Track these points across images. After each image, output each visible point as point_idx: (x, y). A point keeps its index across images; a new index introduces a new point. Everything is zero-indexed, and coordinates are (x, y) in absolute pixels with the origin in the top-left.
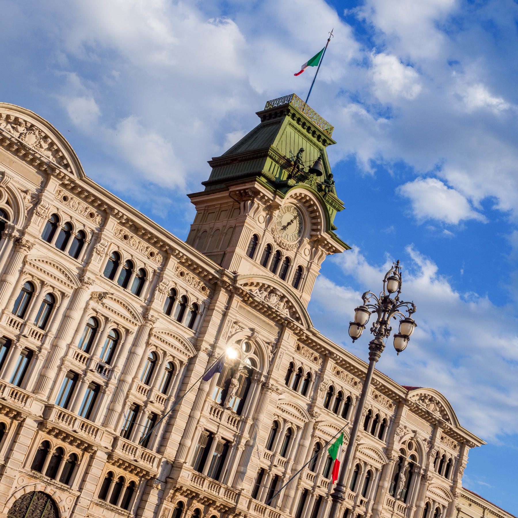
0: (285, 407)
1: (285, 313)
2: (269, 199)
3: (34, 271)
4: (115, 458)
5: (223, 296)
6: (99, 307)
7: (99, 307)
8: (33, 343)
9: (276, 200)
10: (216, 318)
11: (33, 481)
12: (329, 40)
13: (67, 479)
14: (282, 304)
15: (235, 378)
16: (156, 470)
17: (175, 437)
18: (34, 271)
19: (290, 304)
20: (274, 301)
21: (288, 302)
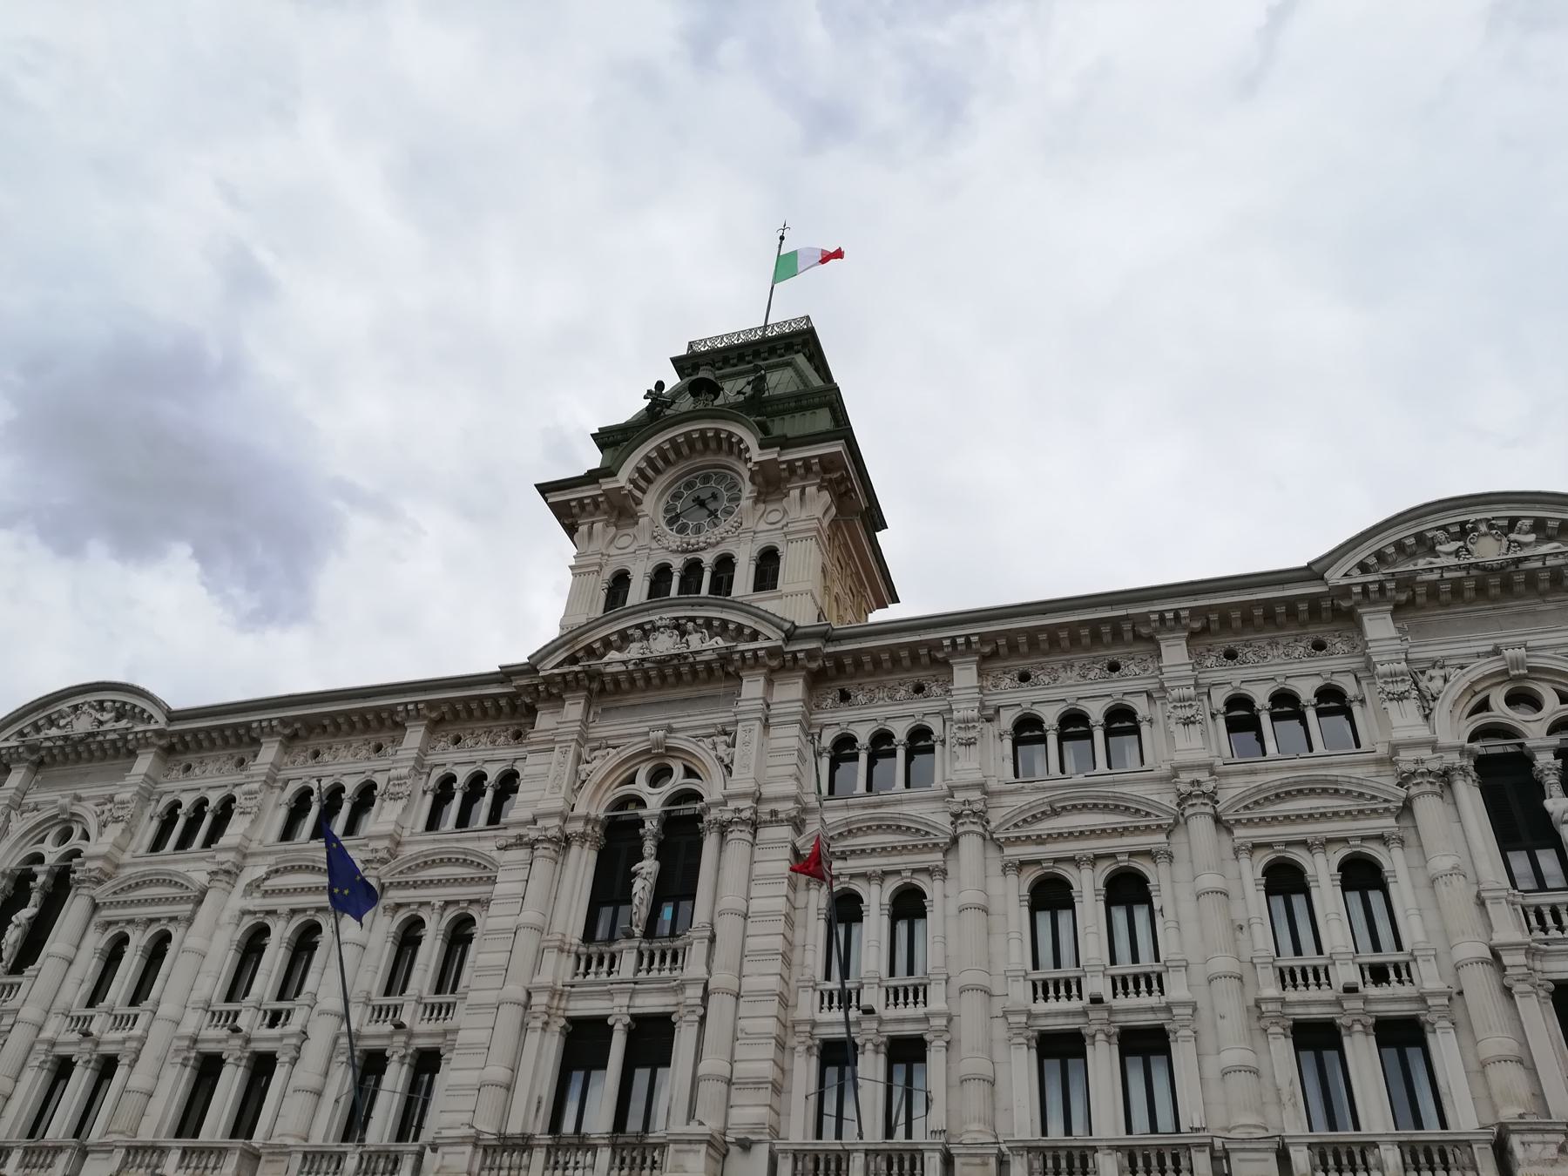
2: (594, 498)
5: (544, 720)
6: (256, 902)
12: (782, 238)
15: (641, 858)
20: (664, 644)
21: (708, 622)
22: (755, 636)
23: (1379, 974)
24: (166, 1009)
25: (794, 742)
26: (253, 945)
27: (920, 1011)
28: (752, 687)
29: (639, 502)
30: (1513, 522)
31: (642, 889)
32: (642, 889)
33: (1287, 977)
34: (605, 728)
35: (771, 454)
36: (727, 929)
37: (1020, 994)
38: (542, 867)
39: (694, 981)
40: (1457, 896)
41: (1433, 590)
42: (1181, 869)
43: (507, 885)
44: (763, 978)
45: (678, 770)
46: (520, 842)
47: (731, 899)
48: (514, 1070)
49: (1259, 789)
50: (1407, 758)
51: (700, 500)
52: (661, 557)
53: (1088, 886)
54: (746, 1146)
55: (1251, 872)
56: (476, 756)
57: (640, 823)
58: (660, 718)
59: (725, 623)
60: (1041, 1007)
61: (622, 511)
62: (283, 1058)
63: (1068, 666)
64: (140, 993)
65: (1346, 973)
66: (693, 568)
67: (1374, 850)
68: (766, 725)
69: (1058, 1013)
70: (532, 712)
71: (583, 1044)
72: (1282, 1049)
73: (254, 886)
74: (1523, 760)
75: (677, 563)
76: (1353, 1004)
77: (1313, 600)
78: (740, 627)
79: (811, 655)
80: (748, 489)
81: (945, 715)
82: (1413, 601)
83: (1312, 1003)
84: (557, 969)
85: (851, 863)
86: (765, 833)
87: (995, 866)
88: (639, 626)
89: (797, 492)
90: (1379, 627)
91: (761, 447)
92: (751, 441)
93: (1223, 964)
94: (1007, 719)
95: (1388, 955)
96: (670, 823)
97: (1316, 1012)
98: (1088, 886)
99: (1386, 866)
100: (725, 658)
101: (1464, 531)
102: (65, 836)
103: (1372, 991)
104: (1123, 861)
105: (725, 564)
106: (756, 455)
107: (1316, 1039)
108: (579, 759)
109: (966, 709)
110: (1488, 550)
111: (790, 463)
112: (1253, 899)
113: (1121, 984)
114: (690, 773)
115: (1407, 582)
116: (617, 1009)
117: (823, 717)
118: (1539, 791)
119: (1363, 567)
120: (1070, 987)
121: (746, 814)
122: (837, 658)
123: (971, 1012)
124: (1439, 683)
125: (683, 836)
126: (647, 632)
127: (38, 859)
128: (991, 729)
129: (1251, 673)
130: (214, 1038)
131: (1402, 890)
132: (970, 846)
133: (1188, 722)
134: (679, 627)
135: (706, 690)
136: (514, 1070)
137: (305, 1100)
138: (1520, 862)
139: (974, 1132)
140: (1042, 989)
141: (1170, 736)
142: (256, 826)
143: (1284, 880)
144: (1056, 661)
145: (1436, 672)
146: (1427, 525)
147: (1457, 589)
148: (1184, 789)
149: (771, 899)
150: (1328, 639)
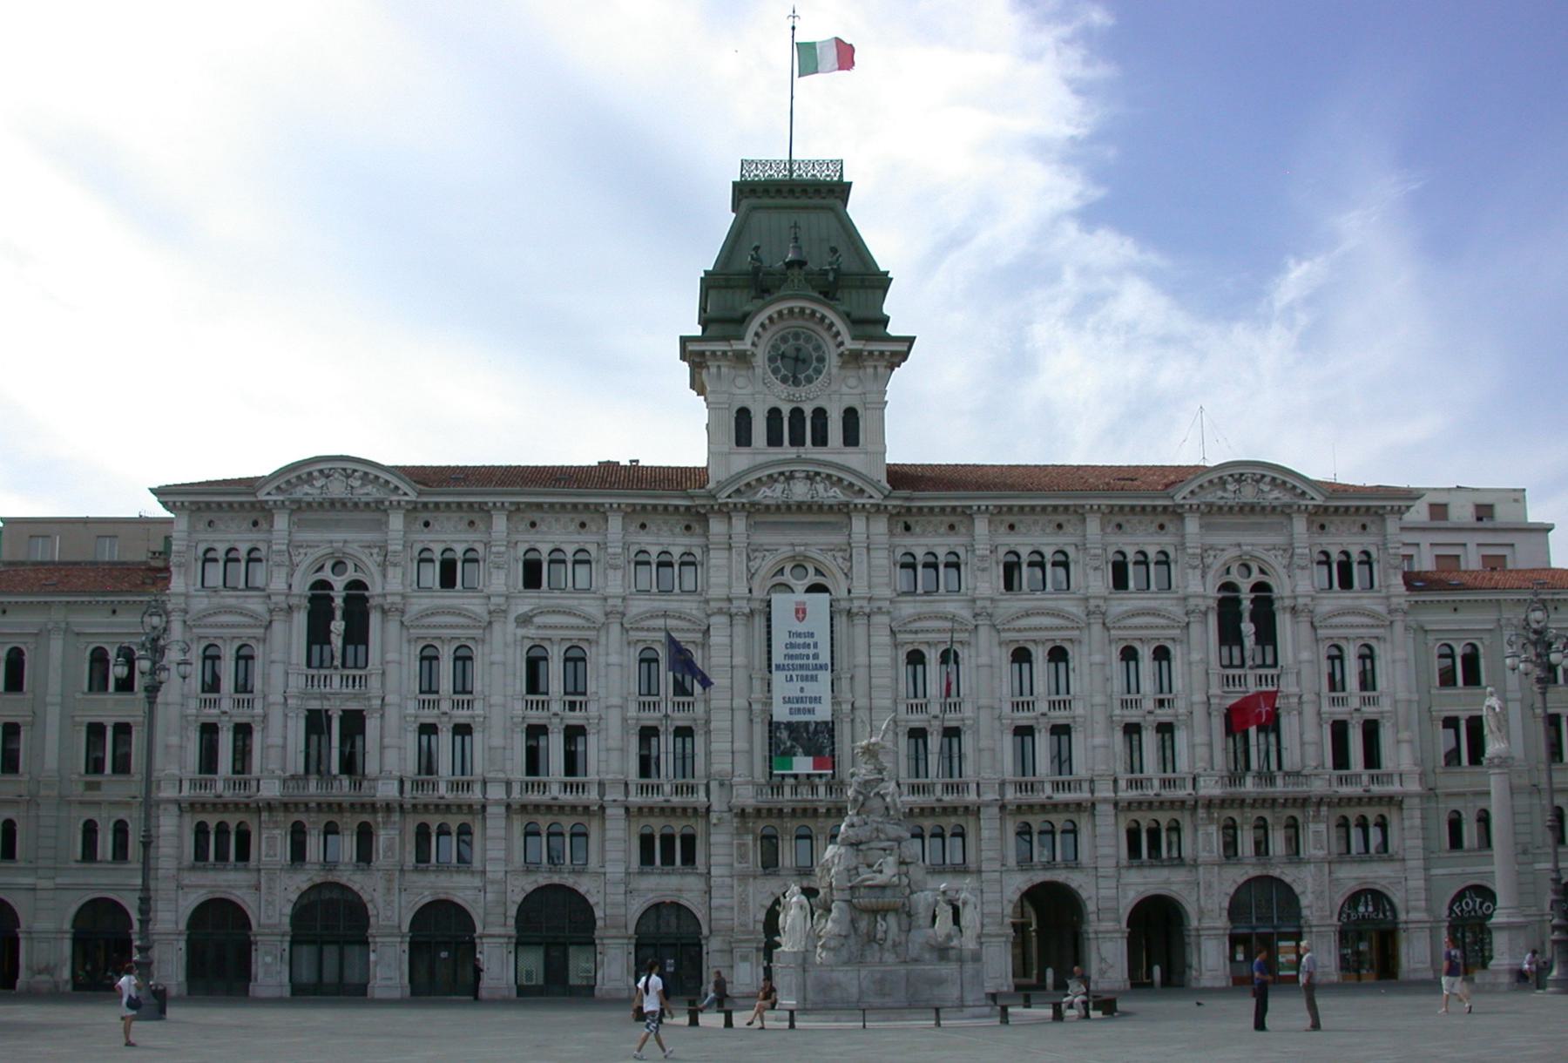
2: (725, 353)
4: (634, 810)
5: (717, 526)
6: (531, 632)
7: (531, 632)
10: (717, 558)
11: (532, 878)
14: (820, 487)
17: (720, 745)
20: (800, 491)
21: (829, 476)
22: (862, 491)
23: (1161, 703)
24: (496, 699)
25: (885, 562)
27: (959, 715)
28: (858, 524)
29: (753, 355)
30: (1263, 476)
33: (1125, 704)
34: (764, 538)
35: (858, 345)
36: (861, 674)
37: (1007, 708)
38: (739, 629)
40: (1198, 671)
41: (1220, 508)
42: (1085, 649)
43: (718, 638)
44: (883, 700)
45: (811, 571)
46: (720, 612)
47: (861, 659)
48: (751, 742)
50: (1192, 602)
51: (795, 363)
53: (1040, 654)
55: (1115, 653)
56: (662, 540)
58: (797, 537)
59: (840, 480)
60: (1016, 715)
61: (743, 358)
62: (591, 730)
63: (1036, 522)
65: (1149, 704)
66: (797, 413)
67: (1169, 645)
68: (868, 549)
69: (1023, 718)
70: (704, 519)
72: (1119, 735)
73: (524, 620)
74: (1237, 602)
75: (786, 410)
76: (1150, 718)
77: (1165, 508)
78: (851, 485)
80: (833, 360)
81: (970, 548)
82: (1211, 513)
83: (1133, 716)
86: (876, 619)
87: (995, 641)
88: (782, 474)
90: (1192, 525)
91: (854, 338)
92: (840, 326)
93: (1098, 699)
95: (1164, 696)
97: (1134, 720)
98: (1040, 654)
99: (1173, 652)
101: (1239, 479)
102: (338, 566)
103: (1158, 711)
105: (820, 414)
106: (850, 345)
107: (1132, 730)
109: (982, 548)
110: (1248, 494)
111: (871, 353)
112: (1117, 666)
113: (1053, 705)
114: (818, 572)
115: (1210, 505)
117: (897, 540)
119: (1192, 492)
120: (1028, 705)
121: (867, 610)
122: (909, 509)
123: (984, 716)
126: (791, 477)
127: (324, 585)
128: (994, 557)
130: (536, 717)
131: (1177, 665)
132: (984, 632)
133: (1096, 569)
134: (810, 478)
135: (824, 518)
136: (751, 742)
137: (615, 755)
138: (1225, 650)
139: (986, 774)
140: (1016, 706)
141: (1086, 575)
143: (1129, 654)
144: (1029, 519)
145: (1212, 553)
146: (1225, 473)
147: (1231, 508)
148: (1092, 608)
149: (882, 657)
150: (1167, 524)
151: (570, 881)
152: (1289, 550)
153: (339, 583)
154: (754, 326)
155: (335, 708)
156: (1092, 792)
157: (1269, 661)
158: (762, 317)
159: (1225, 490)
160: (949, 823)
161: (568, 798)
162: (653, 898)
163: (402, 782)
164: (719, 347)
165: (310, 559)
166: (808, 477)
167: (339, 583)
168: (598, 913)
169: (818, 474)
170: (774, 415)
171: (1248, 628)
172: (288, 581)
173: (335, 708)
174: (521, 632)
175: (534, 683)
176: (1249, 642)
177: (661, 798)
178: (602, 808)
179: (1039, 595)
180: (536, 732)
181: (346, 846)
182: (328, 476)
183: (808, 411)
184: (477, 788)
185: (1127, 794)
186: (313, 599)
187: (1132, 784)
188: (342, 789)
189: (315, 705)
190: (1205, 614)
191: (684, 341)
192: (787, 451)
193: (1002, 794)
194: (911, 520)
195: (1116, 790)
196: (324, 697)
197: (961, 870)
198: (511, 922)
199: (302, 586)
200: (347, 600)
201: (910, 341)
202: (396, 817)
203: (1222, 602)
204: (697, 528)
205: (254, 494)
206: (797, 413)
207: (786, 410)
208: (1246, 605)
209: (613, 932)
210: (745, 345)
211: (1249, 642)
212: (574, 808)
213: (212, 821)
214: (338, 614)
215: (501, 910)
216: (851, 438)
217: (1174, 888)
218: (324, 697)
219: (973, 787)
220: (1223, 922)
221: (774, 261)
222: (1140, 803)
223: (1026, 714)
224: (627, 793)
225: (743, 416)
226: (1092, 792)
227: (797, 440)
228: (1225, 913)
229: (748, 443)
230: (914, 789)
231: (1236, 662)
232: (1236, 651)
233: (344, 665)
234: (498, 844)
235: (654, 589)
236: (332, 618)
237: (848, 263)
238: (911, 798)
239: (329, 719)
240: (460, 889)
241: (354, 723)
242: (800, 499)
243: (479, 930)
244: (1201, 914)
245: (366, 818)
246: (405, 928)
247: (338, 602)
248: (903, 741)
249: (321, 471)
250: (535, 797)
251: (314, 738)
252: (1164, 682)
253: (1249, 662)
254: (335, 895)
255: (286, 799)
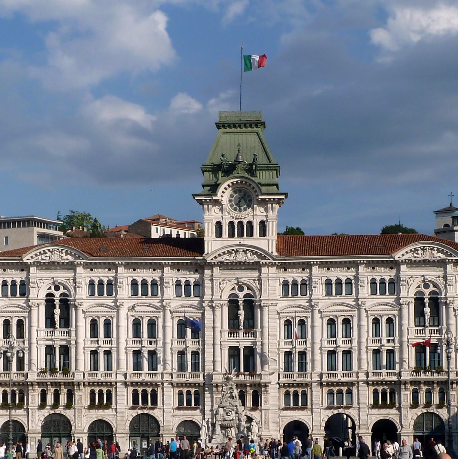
0: (289, 310)
1: (256, 259)
3: (91, 314)
4: (175, 384)
6: (134, 314)
7: (134, 314)
8: (107, 347)
9: (214, 198)
10: (207, 284)
13: (154, 402)
14: (249, 255)
15: (240, 310)
16: (201, 379)
17: (209, 358)
18: (91, 314)
19: (254, 252)
20: (241, 257)
21: (252, 251)
23: (389, 341)
26: (137, 324)
30: (434, 247)
31: (242, 318)
32: (242, 318)
39: (259, 341)
49: (374, 304)
52: (231, 219)
54: (273, 373)
57: (238, 302)
61: (217, 203)
64: (108, 334)
66: (241, 223)
71: (234, 352)
75: (236, 222)
79: (279, 263)
84: (226, 336)
85: (289, 314)
88: (233, 250)
89: (270, 205)
92: (256, 188)
94: (324, 279)
96: (244, 301)
100: (257, 263)
104: (347, 317)
105: (250, 223)
108: (220, 284)
116: (242, 345)
118: (424, 306)
124: (412, 281)
125: (250, 305)
126: (237, 251)
129: (377, 274)
134: (245, 252)
142: (124, 291)
151: (151, 412)
152: (445, 278)
153: (57, 294)
154: (221, 189)
155: (57, 345)
156: (358, 377)
157: (436, 324)
158: (225, 185)
159: (418, 254)
160: (300, 390)
161: (149, 379)
162: (183, 419)
163: (84, 374)
164: (208, 199)
165: (46, 284)
166: (243, 251)
167: (57, 294)
168: (161, 424)
169: (247, 250)
170: (231, 224)
171: (427, 310)
172: (39, 293)
173: (57, 345)
174: (130, 313)
175: (137, 333)
176: (428, 316)
177: (185, 380)
178: (163, 384)
179: (338, 297)
180: (137, 354)
181: (63, 399)
182: (51, 252)
183: (245, 222)
184: (114, 376)
185: (372, 378)
186: (46, 301)
187: (375, 374)
188: (59, 377)
189: (50, 343)
190: (408, 305)
191: (194, 196)
192: (236, 240)
193: (321, 378)
194: (285, 266)
195: (367, 377)
196: (52, 340)
197: (304, 407)
198: (127, 428)
199: (43, 295)
200: (60, 301)
201: (286, 195)
202: (82, 387)
203: (416, 299)
204: (200, 271)
205: (22, 259)
206: (241, 223)
207: (236, 222)
208: (427, 300)
209: (167, 432)
210: (218, 197)
211: (428, 316)
212: (151, 383)
213: (8, 389)
214: (57, 306)
215: (123, 423)
216: (263, 233)
217: (391, 416)
218: (52, 340)
219: (309, 375)
220: (411, 430)
221: (230, 159)
222: (377, 382)
223: (333, 345)
224: (172, 378)
225: (219, 224)
226: (358, 377)
227: (241, 235)
228: (412, 427)
229: (221, 236)
230: (286, 376)
231: (422, 324)
232: (422, 319)
233: (60, 327)
234: (123, 397)
235: (183, 296)
236: (55, 308)
237: (262, 160)
238: (284, 380)
239: (55, 348)
240: (107, 415)
241: (65, 350)
242: (240, 260)
243: (114, 431)
244: (402, 427)
245: (70, 388)
246: (86, 431)
247: (57, 302)
248: (282, 357)
249: (49, 250)
250: (136, 379)
251: (48, 356)
252: (391, 333)
253: (427, 324)
254: (58, 418)
255: (39, 381)
